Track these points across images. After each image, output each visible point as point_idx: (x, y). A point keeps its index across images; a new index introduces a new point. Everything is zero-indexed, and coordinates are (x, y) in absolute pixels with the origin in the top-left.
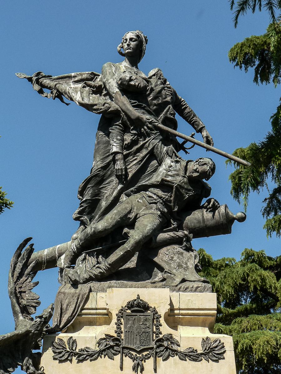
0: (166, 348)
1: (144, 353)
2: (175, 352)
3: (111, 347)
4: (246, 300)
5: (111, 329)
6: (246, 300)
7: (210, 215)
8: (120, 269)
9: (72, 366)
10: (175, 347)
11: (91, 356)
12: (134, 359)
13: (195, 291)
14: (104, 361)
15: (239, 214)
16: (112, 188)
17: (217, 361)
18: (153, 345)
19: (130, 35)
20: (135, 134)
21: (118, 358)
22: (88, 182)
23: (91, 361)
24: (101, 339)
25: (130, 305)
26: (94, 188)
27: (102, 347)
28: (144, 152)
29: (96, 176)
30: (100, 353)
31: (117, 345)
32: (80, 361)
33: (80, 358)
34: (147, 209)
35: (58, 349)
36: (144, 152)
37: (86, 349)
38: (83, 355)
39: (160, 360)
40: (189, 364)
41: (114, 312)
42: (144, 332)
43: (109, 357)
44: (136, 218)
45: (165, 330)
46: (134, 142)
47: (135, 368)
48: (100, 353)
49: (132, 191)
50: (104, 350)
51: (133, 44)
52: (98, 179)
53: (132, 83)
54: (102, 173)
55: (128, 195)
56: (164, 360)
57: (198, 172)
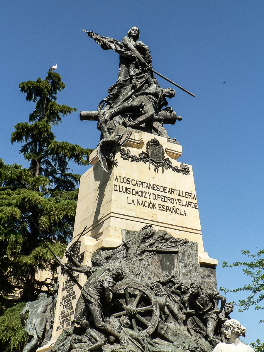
0: (167, 164)
1: (159, 164)
2: (171, 167)
3: (145, 158)
4: (4, 185)
5: (144, 149)
6: (4, 185)
7: (170, 114)
8: (141, 126)
9: (129, 162)
10: (171, 164)
11: (137, 160)
12: (155, 166)
13: (173, 143)
14: (141, 163)
15: (180, 117)
16: (128, 91)
17: (187, 175)
18: (162, 161)
19: (135, 28)
20: (141, 70)
21: (148, 163)
22: (116, 85)
23: (137, 162)
24: (141, 153)
25: (152, 141)
26: (118, 89)
27: (142, 157)
28: (143, 79)
29: (121, 84)
30: (141, 159)
31: (147, 157)
32: (132, 161)
33: (133, 159)
34: (149, 103)
35: (123, 153)
36: (143, 79)
37: (134, 156)
38: (134, 158)
39: (165, 168)
40: (176, 173)
41: (146, 143)
42: (158, 155)
43: (144, 162)
44: (144, 106)
45: (166, 156)
46: (140, 73)
47: (155, 170)
48: (141, 159)
49: (139, 94)
50: (142, 158)
51: (137, 32)
52: (121, 85)
53: (143, 47)
54: (123, 83)
55: (136, 96)
56: (166, 169)
57: (169, 93)
